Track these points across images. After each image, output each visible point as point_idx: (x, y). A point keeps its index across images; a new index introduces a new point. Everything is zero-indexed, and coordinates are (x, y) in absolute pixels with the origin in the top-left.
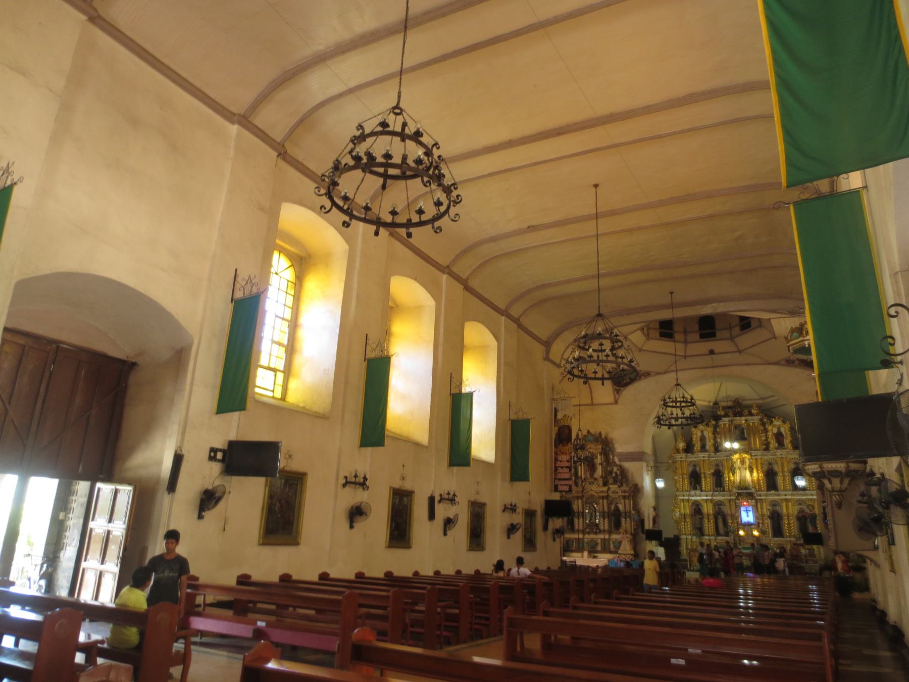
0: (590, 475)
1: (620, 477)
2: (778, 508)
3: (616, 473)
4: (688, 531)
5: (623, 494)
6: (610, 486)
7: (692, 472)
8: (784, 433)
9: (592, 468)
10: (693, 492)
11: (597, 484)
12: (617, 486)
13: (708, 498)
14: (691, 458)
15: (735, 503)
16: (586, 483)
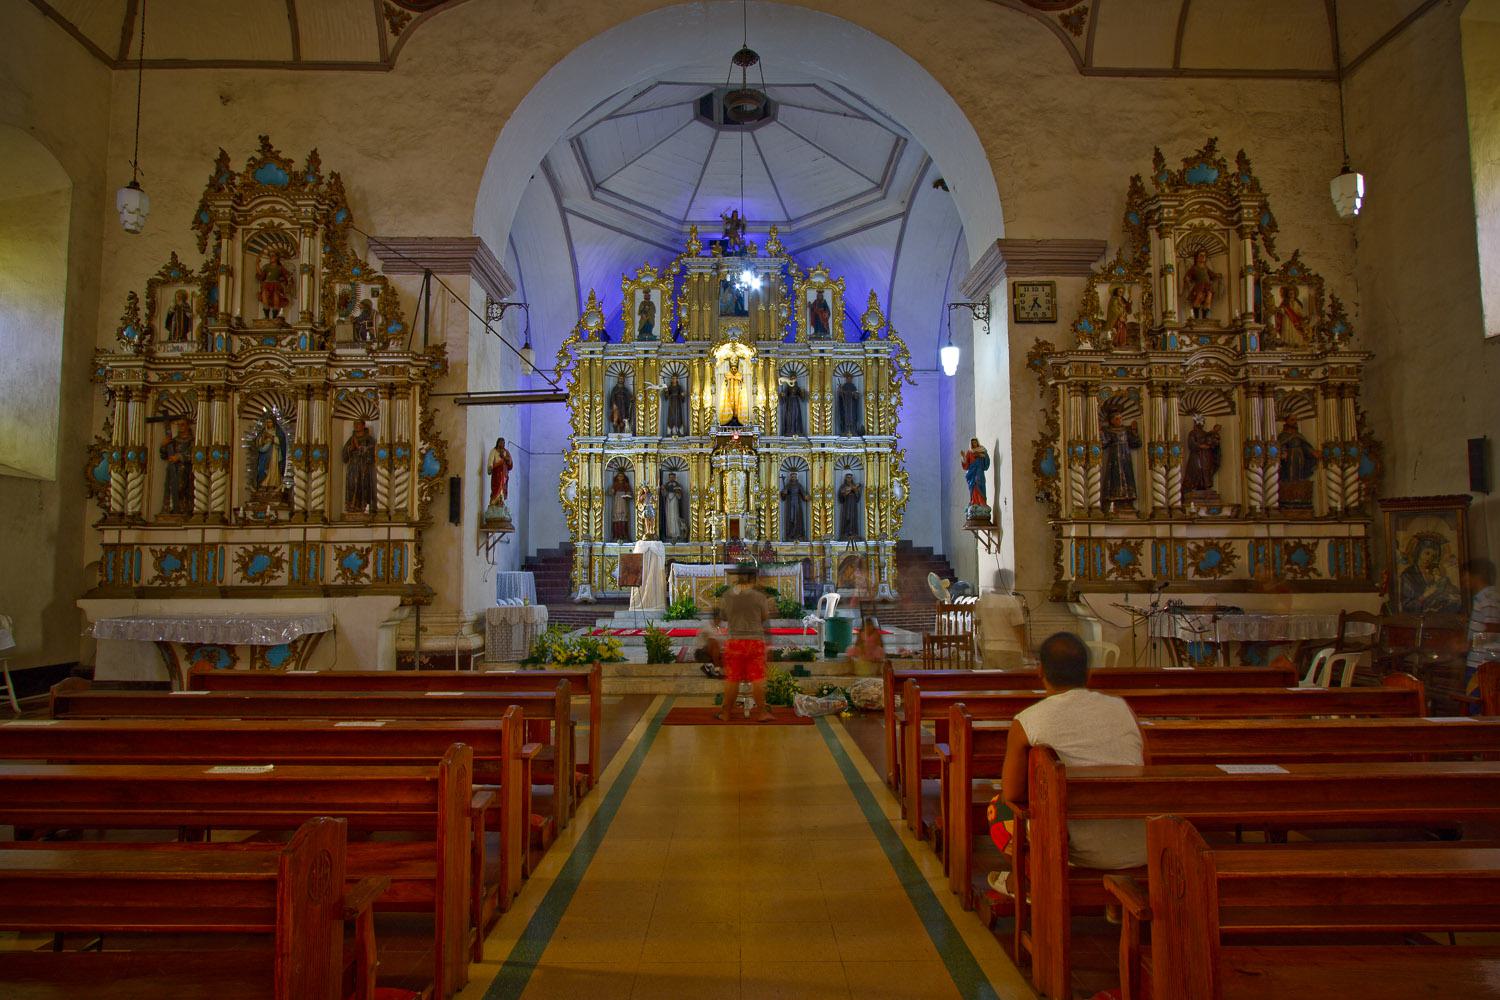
0: (267, 312)
1: (380, 320)
2: (801, 476)
3: (366, 305)
4: (596, 531)
5: (388, 379)
6: (338, 352)
7: (615, 389)
8: (830, 304)
9: (276, 286)
10: (613, 437)
11: (291, 343)
12: (362, 351)
13: (649, 450)
14: (618, 353)
15: (711, 463)
16: (248, 343)
